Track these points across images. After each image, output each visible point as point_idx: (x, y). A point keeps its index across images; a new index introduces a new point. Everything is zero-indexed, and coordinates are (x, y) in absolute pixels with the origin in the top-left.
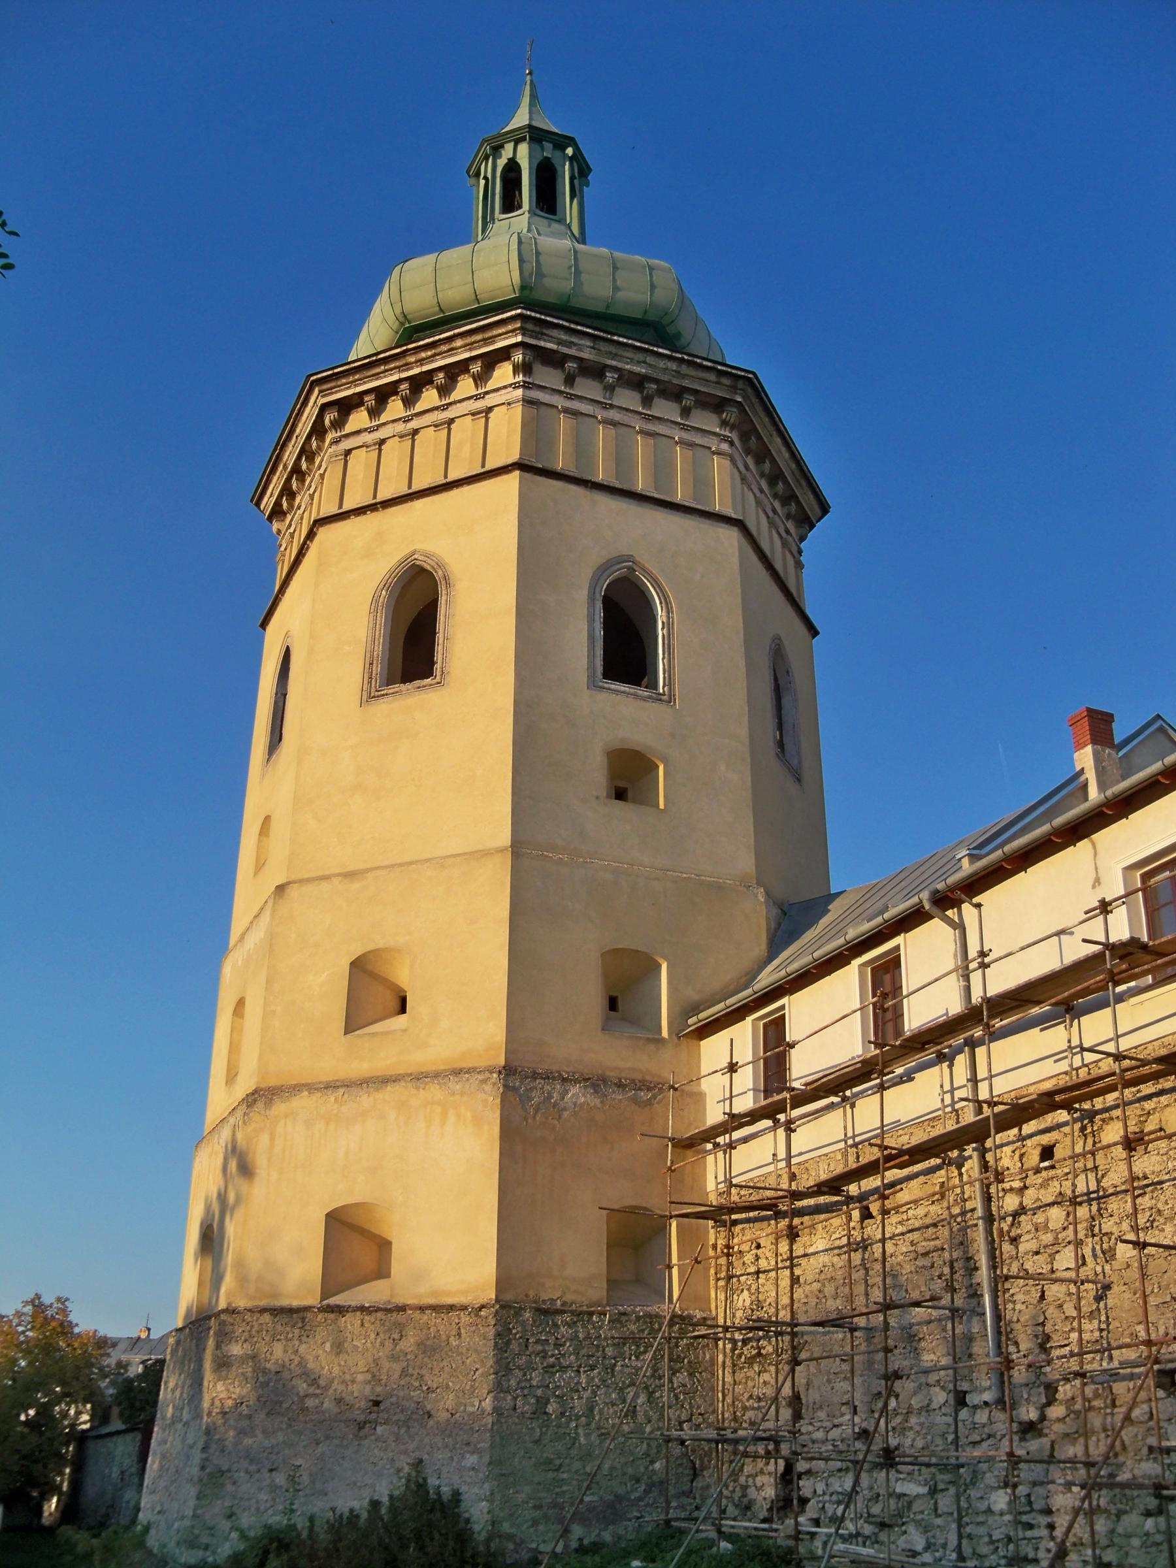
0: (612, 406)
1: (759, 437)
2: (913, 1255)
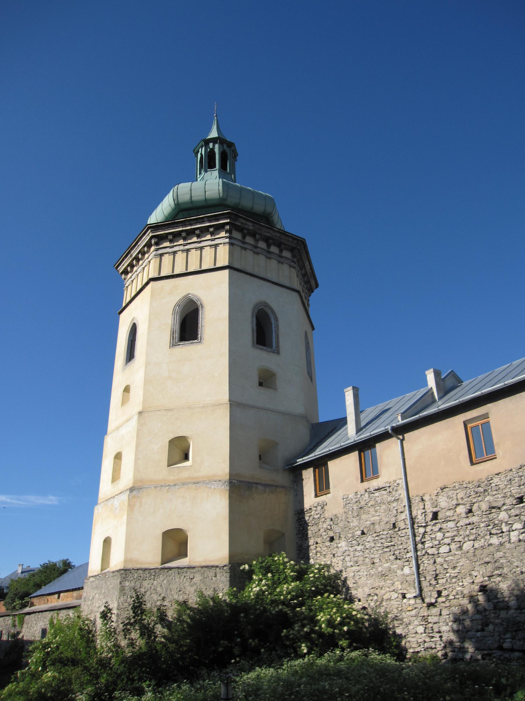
1: (303, 261)
2: (382, 547)
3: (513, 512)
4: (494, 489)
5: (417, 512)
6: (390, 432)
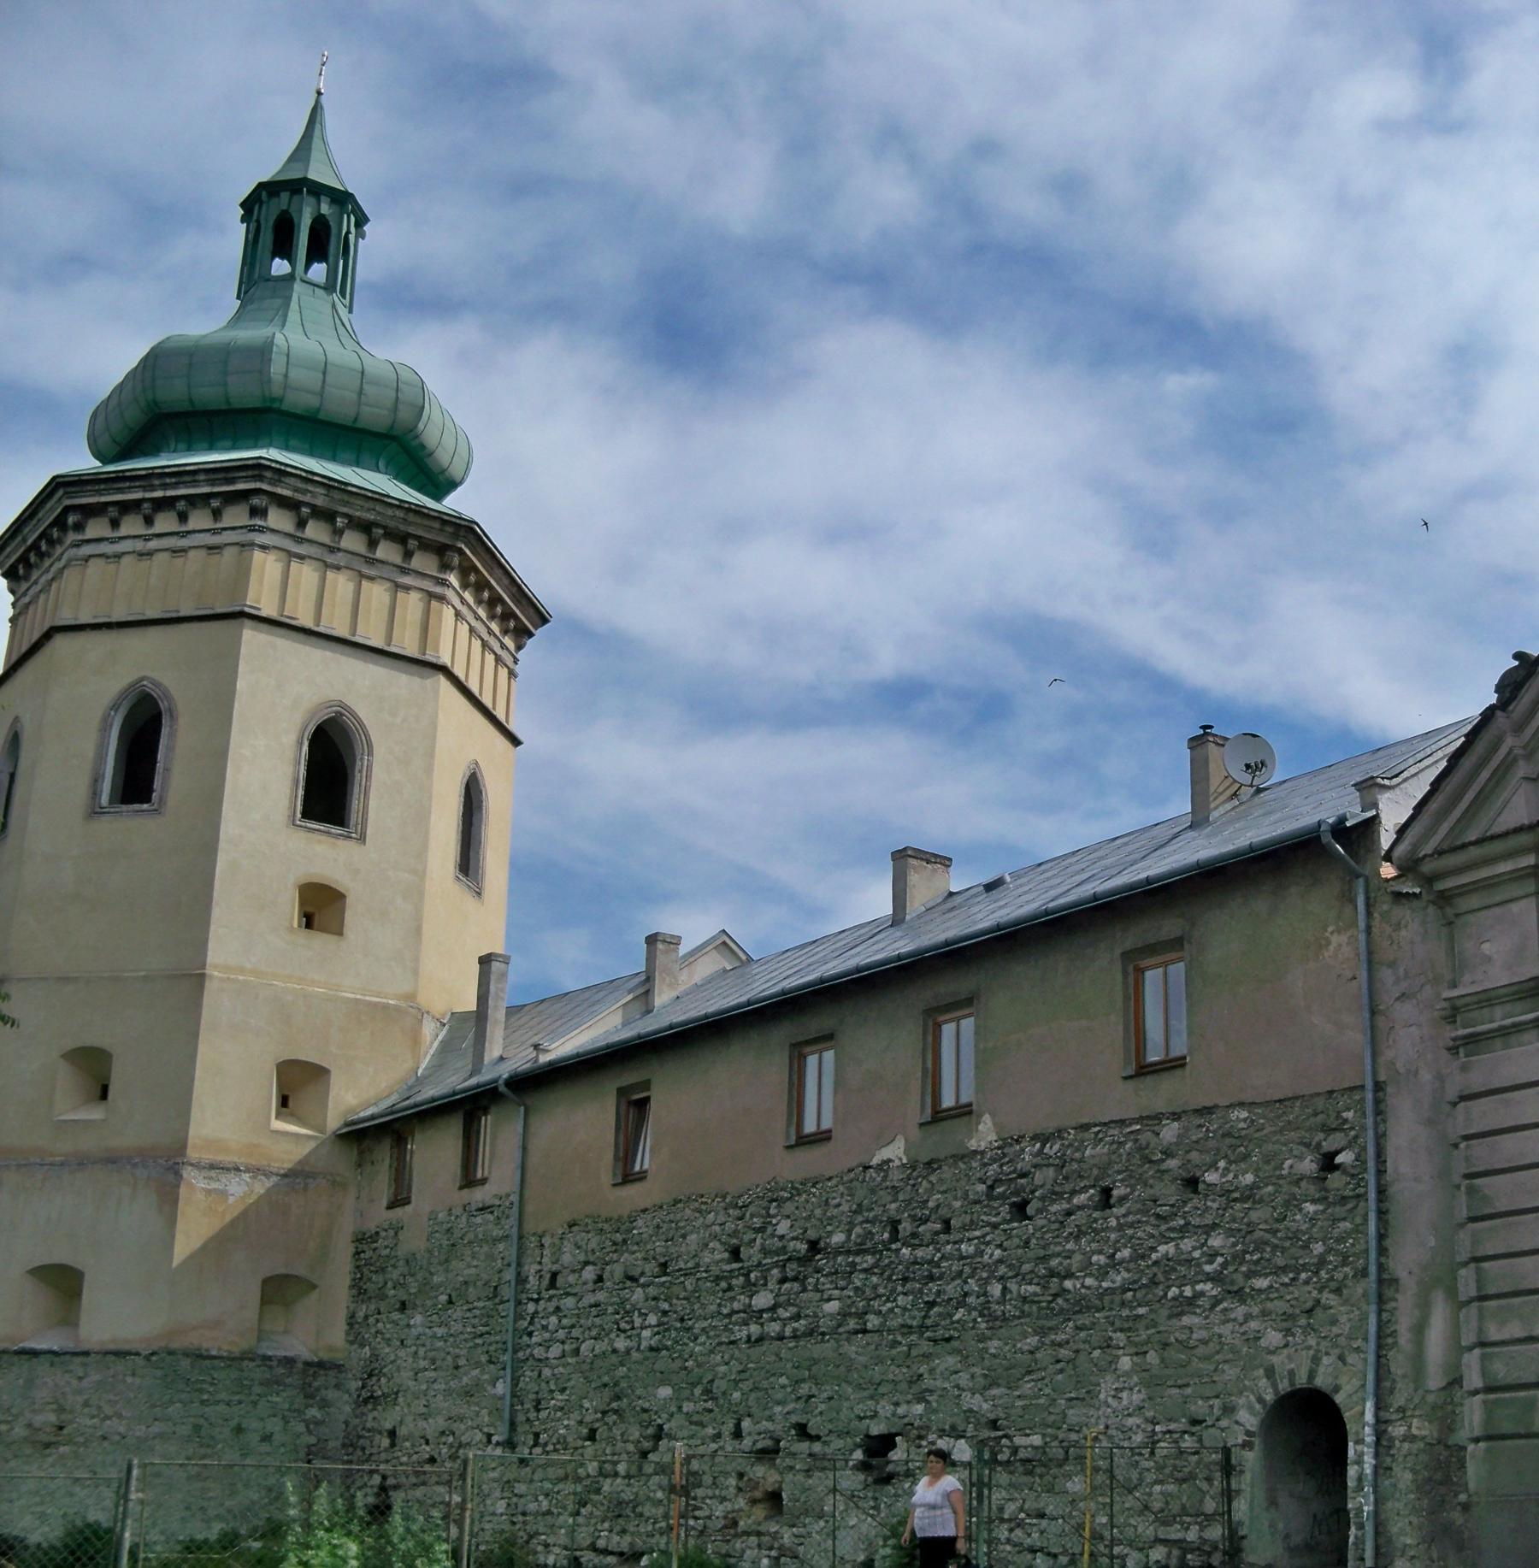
0: (339, 550)
3: (652, 1291)
4: (637, 1239)
5: (531, 1269)
6: (502, 1089)
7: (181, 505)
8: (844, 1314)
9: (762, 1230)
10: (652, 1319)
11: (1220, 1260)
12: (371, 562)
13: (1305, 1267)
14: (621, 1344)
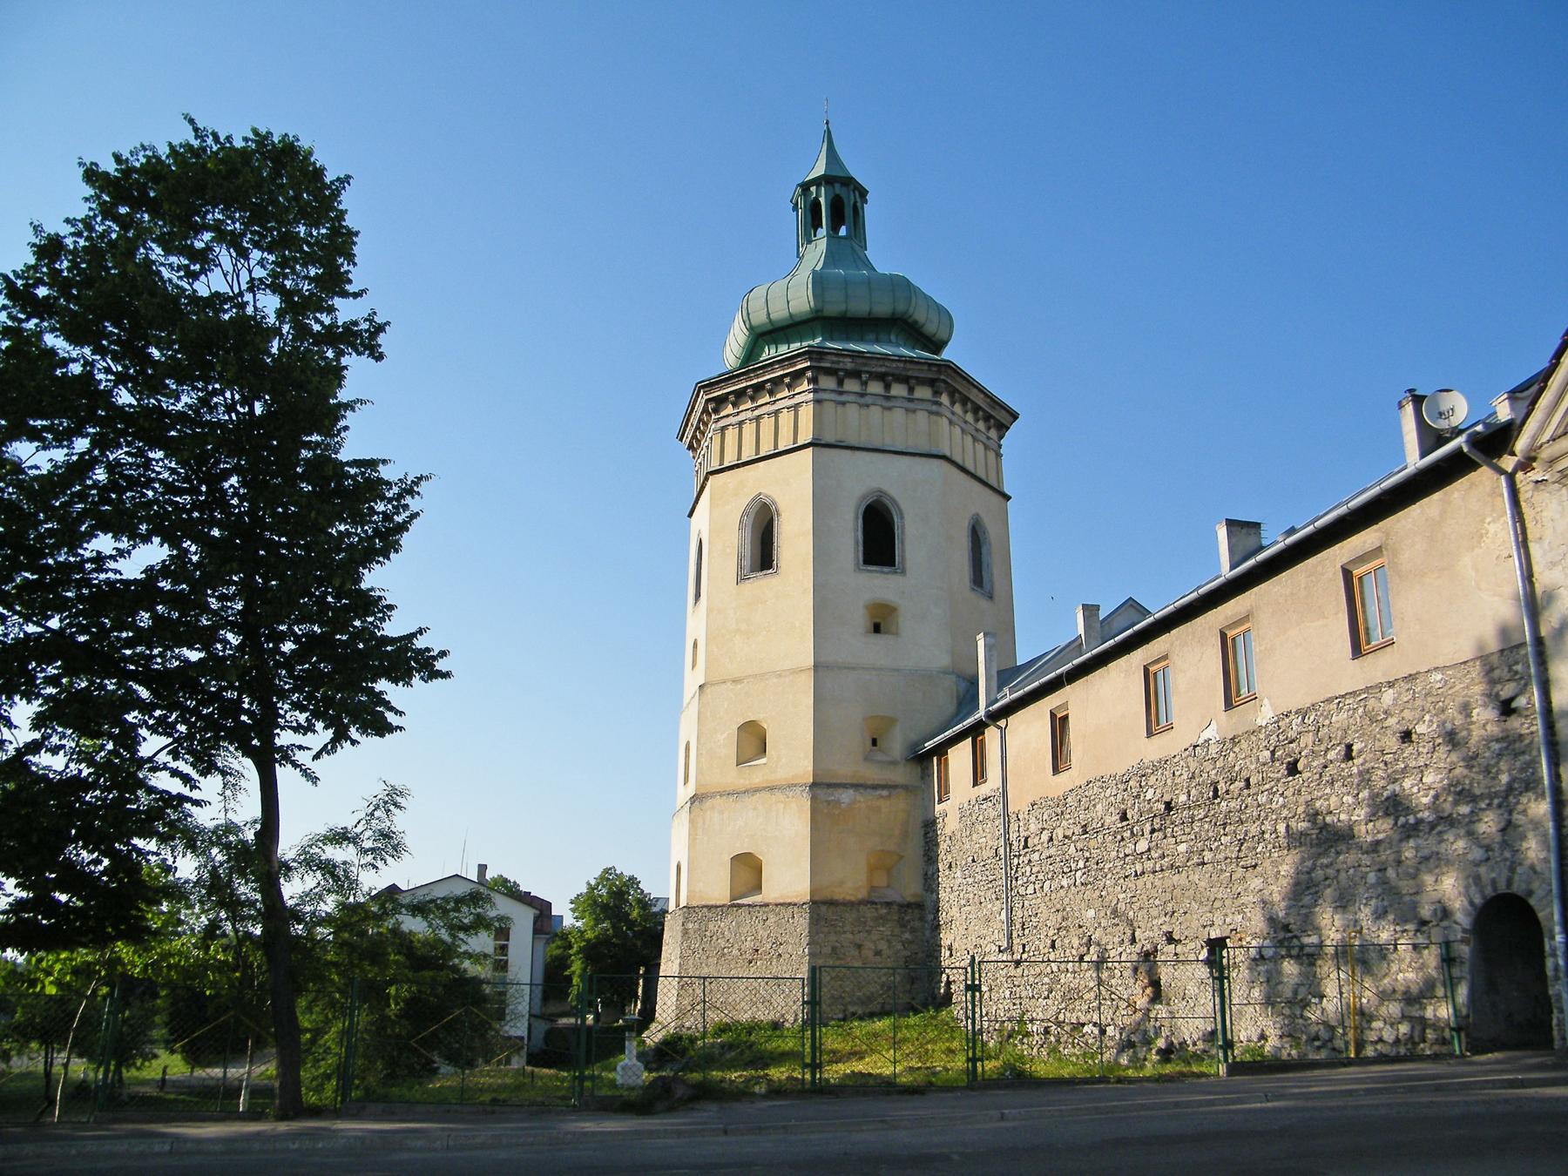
3: (1080, 846)
5: (1013, 836)
7: (768, 386)
8: (1190, 852)
9: (1138, 796)
10: (1081, 864)
11: (1432, 792)
12: (888, 398)
13: (1496, 795)
14: (1065, 883)
